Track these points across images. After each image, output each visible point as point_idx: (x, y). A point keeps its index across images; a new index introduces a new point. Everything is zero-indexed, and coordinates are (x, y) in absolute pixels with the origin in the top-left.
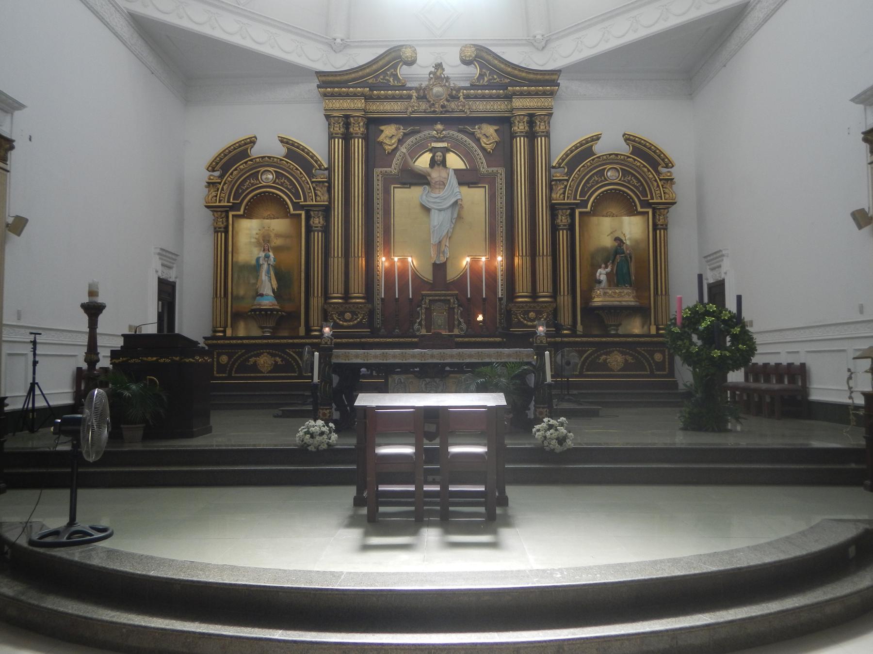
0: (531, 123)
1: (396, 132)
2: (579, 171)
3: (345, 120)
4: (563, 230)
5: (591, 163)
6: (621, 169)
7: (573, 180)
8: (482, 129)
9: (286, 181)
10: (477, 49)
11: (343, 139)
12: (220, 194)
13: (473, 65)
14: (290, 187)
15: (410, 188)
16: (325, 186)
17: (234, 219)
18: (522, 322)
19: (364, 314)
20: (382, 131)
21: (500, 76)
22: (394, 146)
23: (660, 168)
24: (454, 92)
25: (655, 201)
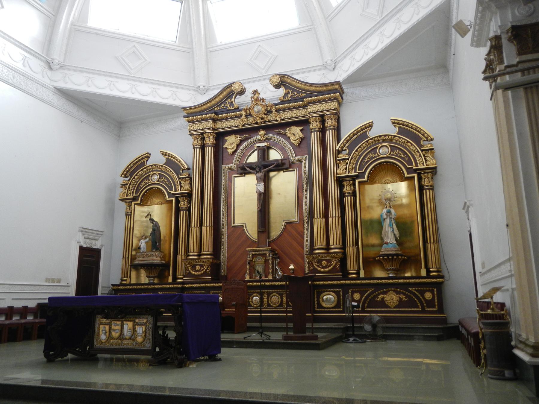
2: (357, 151)
4: (348, 196)
5: (365, 144)
6: (390, 146)
7: (352, 158)
10: (280, 77)
12: (128, 191)
13: (281, 88)
14: (167, 183)
15: (244, 176)
16: (188, 180)
17: (136, 205)
18: (316, 269)
19: (208, 266)
21: (299, 92)
23: (422, 142)
24: (269, 108)
25: (419, 167)
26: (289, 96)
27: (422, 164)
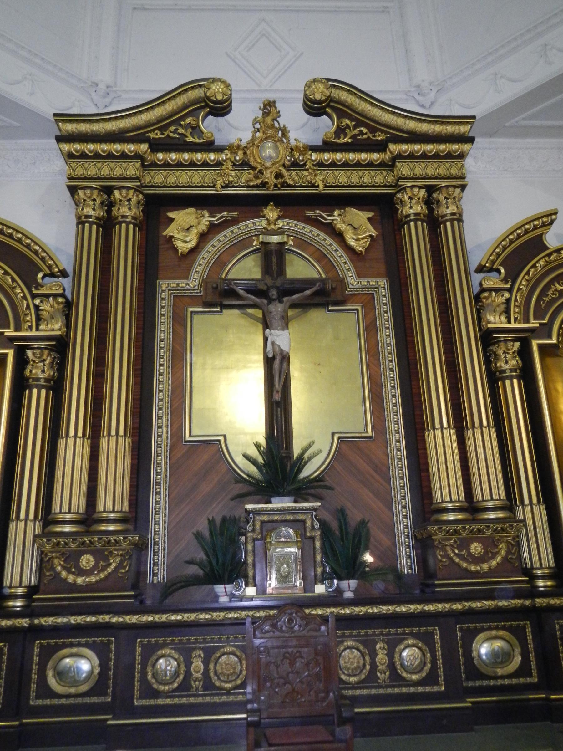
1: (196, 221)
2: (528, 273)
3: (105, 196)
4: (511, 378)
11: (98, 226)
13: (325, 117)
15: (221, 312)
18: (458, 565)
19: (121, 555)
20: (172, 220)
21: (373, 130)
26: (350, 134)
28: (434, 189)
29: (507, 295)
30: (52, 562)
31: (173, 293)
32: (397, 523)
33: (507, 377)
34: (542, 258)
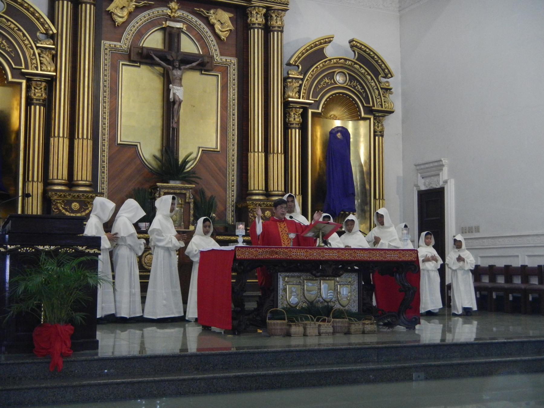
0: (267, 16)
1: (127, 3)
2: (313, 71)
4: (295, 128)
6: (349, 74)
7: (307, 80)
8: (217, 15)
9: (4, 42)
15: (139, 67)
22: (126, 17)
25: (376, 108)
27: (379, 105)
28: (270, 9)
29: (300, 82)
30: (57, 205)
31: (112, 50)
32: (228, 199)
33: (293, 128)
34: (321, 63)
